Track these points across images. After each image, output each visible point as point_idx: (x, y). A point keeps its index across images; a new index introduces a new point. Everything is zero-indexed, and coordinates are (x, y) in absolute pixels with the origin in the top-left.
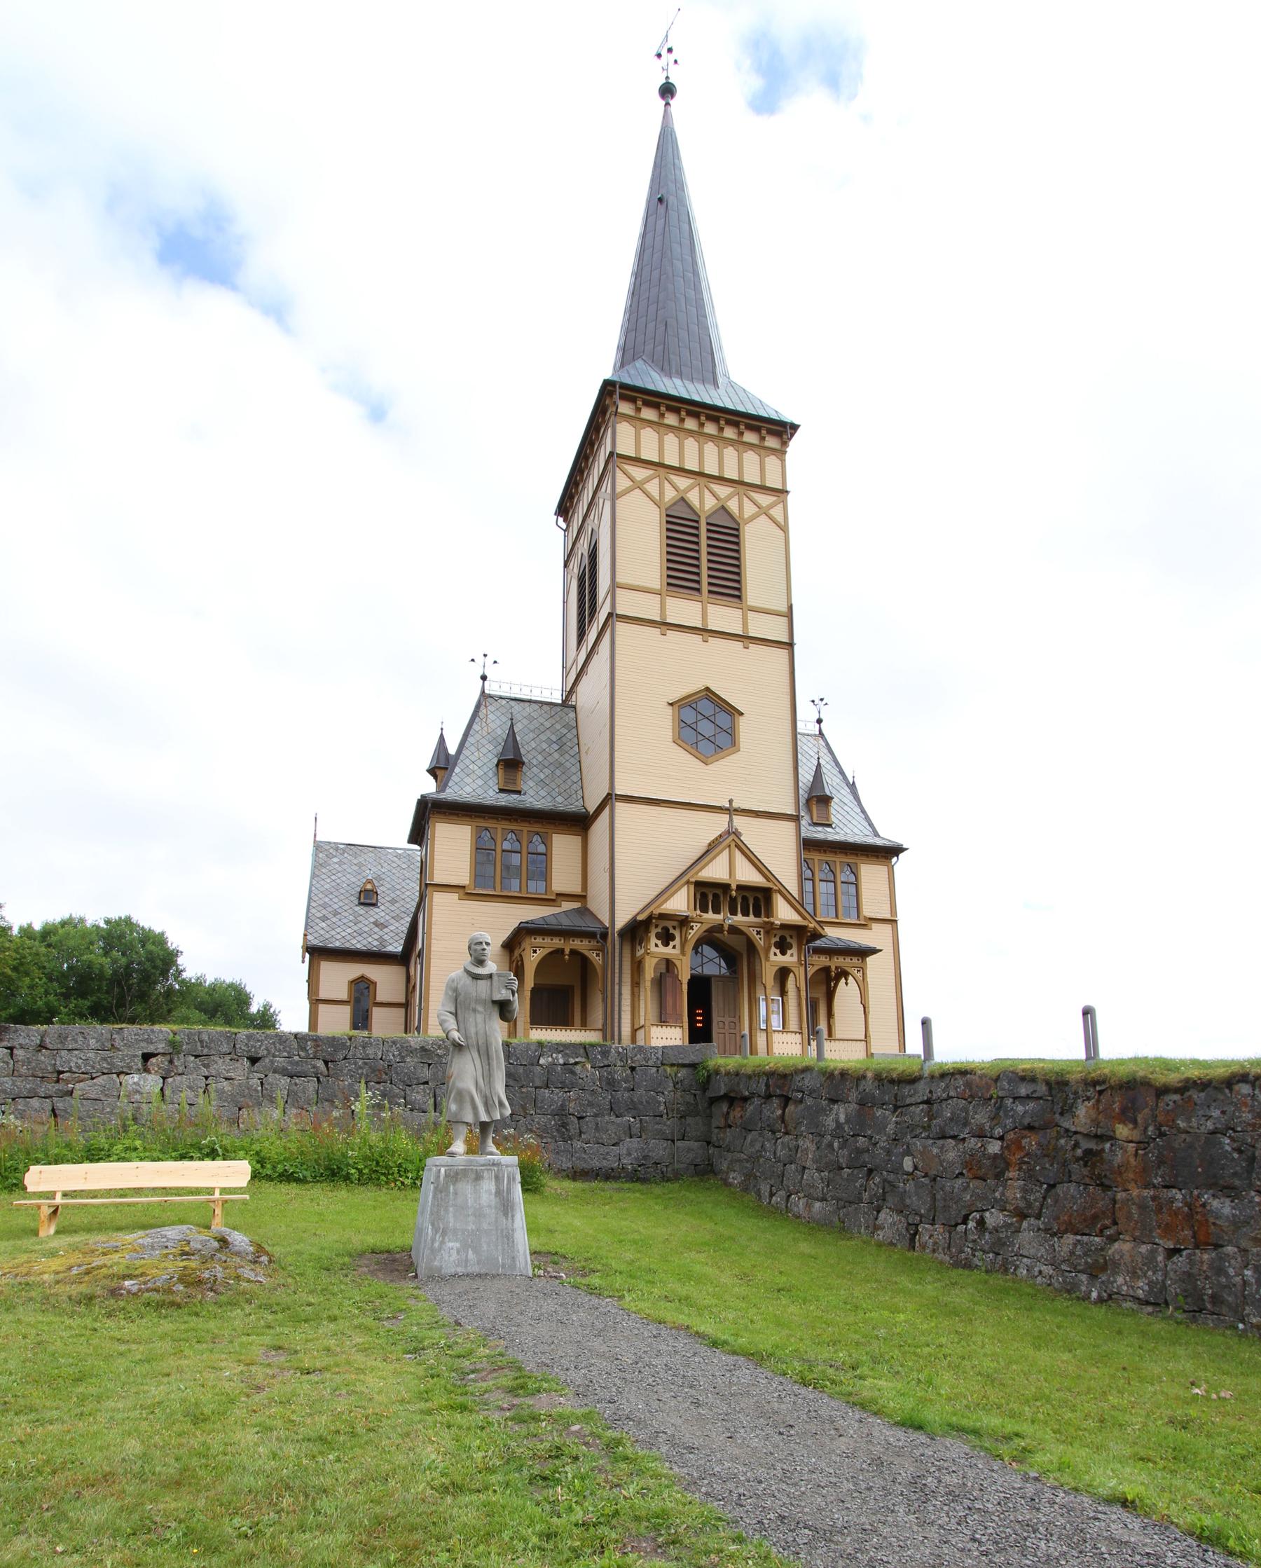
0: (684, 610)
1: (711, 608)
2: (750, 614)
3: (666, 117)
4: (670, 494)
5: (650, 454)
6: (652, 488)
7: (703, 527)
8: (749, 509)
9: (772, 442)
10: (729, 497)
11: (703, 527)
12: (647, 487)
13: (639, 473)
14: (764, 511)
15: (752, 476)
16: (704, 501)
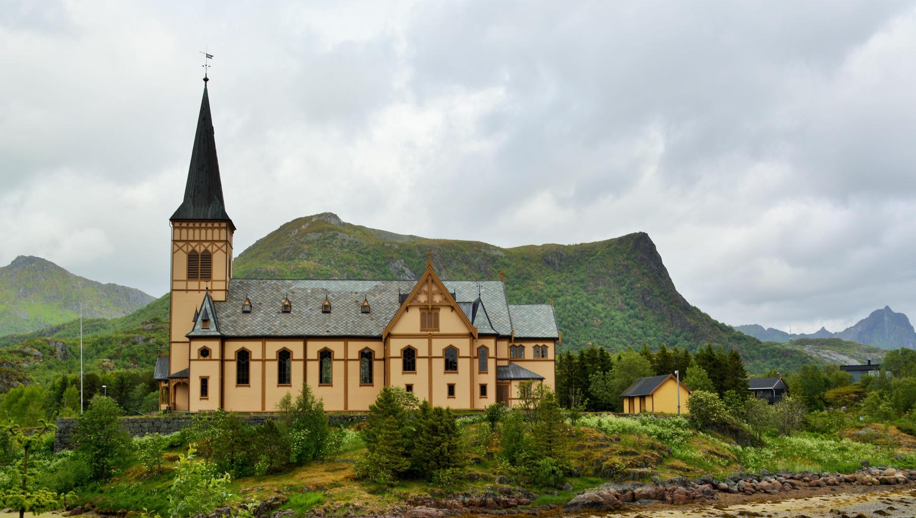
0: (193, 285)
1: (201, 282)
2: (213, 282)
3: (206, 85)
4: (190, 249)
5: (184, 238)
6: (185, 248)
7: (200, 257)
8: (215, 248)
9: (224, 225)
10: (209, 246)
11: (200, 257)
12: (183, 248)
13: (180, 244)
14: (220, 248)
15: (216, 238)
16: (200, 249)
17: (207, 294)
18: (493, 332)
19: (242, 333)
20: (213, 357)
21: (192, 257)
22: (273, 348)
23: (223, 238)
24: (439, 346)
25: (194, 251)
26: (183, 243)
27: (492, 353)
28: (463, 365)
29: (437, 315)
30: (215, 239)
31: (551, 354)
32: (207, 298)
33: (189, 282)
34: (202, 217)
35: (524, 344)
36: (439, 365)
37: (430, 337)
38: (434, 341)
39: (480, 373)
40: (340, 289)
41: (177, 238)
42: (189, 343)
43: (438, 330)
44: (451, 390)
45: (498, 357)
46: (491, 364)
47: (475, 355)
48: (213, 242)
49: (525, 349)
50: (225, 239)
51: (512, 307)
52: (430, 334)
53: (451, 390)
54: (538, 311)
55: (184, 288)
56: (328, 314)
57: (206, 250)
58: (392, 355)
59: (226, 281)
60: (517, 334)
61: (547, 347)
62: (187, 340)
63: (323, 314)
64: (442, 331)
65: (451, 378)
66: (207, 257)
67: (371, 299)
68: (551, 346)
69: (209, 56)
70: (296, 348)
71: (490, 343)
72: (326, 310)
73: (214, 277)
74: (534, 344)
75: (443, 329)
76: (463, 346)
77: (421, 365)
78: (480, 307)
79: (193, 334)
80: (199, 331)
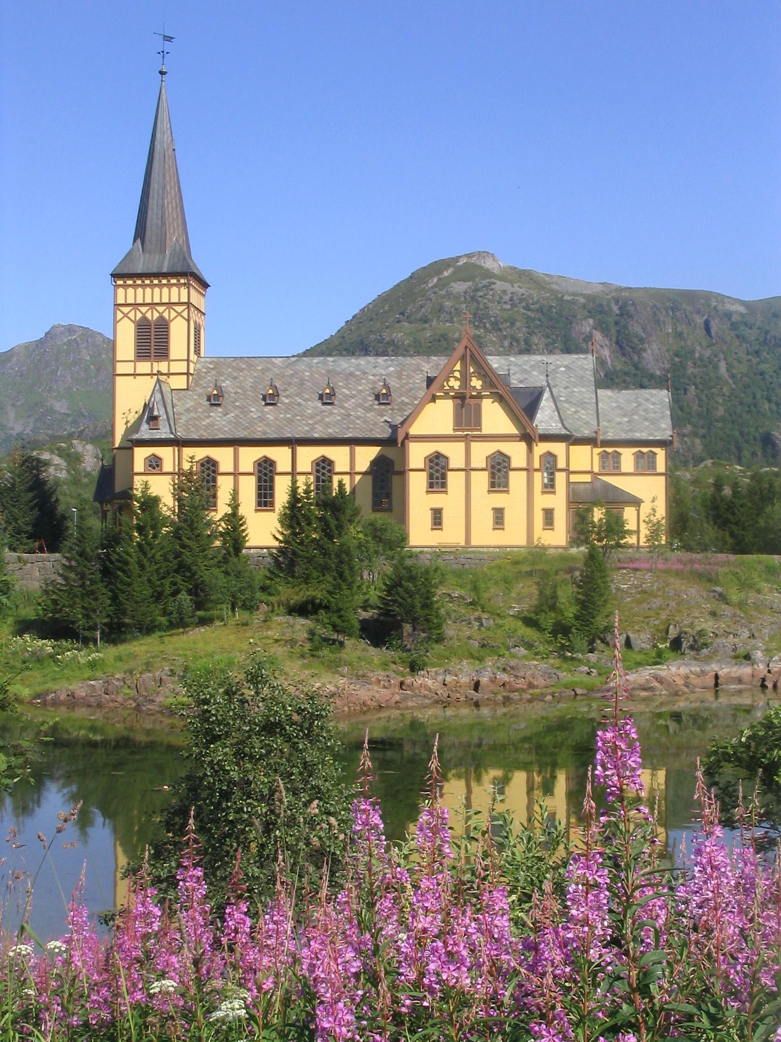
0: (144, 367)
4: (139, 316)
5: (131, 300)
6: (132, 315)
8: (173, 314)
11: (153, 327)
13: (126, 310)
14: (179, 314)
15: (174, 299)
16: (152, 315)
17: (158, 381)
18: (564, 432)
19: (206, 435)
20: (165, 470)
21: (143, 327)
22: (250, 456)
23: (184, 299)
24: (481, 452)
25: (144, 318)
26: (129, 308)
27: (561, 464)
28: (517, 480)
29: (478, 409)
30: (172, 301)
31: (661, 466)
32: (158, 386)
33: (138, 364)
34: (155, 270)
35: (619, 450)
36: (481, 480)
37: (467, 440)
38: (473, 444)
39: (543, 493)
40: (352, 369)
41: (121, 300)
42: (131, 449)
43: (480, 430)
44: (499, 516)
45: (571, 469)
46: (560, 478)
47: (537, 465)
48: (170, 305)
49: (622, 457)
50: (186, 300)
51: (602, 393)
52: (467, 435)
53: (499, 516)
54: (647, 400)
55: (132, 372)
56: (329, 407)
57: (161, 317)
58: (412, 466)
59: (188, 360)
60: (610, 436)
61: (656, 454)
62: (129, 444)
63: (324, 407)
64: (486, 429)
65: (499, 500)
66: (163, 326)
67: (393, 383)
68: (661, 454)
69: (168, 39)
70: (281, 456)
71: (558, 448)
72: (327, 399)
73: (172, 356)
74: (636, 450)
75: (486, 429)
76: (517, 452)
77: (455, 480)
78: (546, 395)
79: (135, 437)
80: (145, 432)
